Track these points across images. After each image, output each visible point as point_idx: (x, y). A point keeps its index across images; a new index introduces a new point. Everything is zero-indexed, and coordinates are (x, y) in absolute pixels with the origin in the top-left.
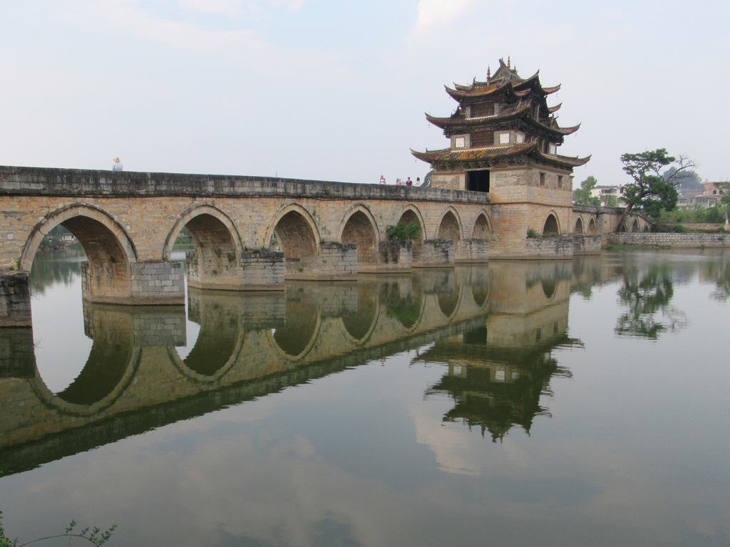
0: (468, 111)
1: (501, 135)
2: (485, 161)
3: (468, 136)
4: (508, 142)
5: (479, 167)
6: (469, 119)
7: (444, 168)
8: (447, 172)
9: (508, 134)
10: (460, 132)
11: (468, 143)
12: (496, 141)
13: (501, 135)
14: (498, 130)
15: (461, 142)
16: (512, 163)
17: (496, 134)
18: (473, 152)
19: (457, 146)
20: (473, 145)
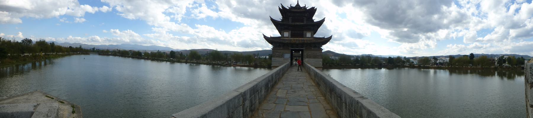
1: (307, 33)
2: (297, 45)
4: (310, 37)
5: (297, 48)
6: (290, 23)
9: (310, 33)
11: (290, 35)
13: (307, 33)
14: (306, 30)
15: (286, 34)
16: (315, 47)
17: (305, 32)
19: (284, 36)
20: (293, 35)
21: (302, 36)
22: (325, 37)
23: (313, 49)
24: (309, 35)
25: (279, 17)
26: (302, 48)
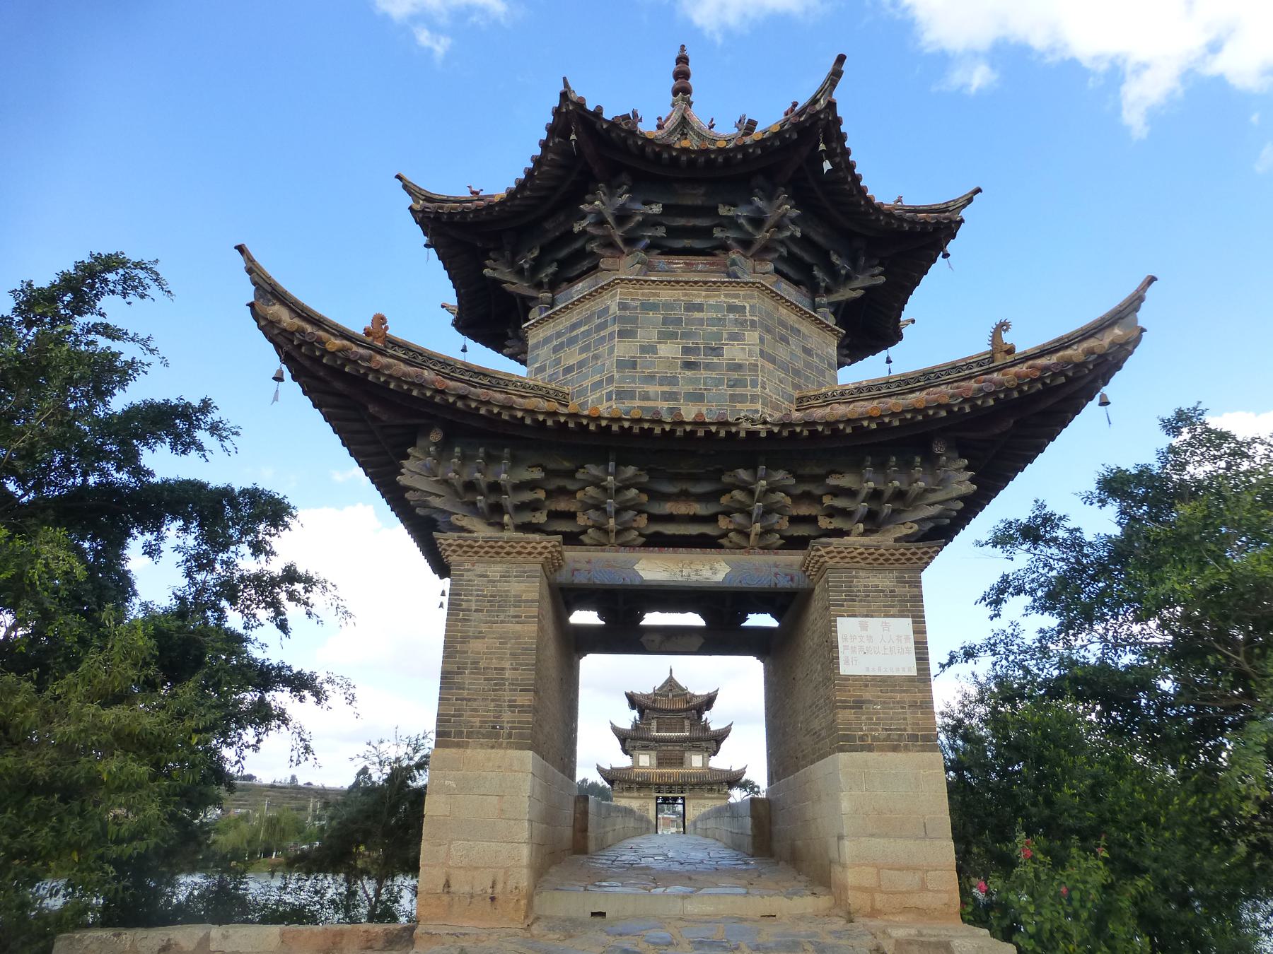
0: (654, 723)
3: (654, 754)
5: (670, 792)
7: (629, 789)
8: (632, 795)
10: (645, 748)
11: (654, 762)
12: (687, 762)
14: (690, 750)
15: (645, 760)
16: (711, 790)
18: (662, 775)
20: (661, 762)
21: (681, 762)
22: (733, 769)
23: (706, 795)
24: (696, 761)
25: (627, 718)
26: (682, 792)
